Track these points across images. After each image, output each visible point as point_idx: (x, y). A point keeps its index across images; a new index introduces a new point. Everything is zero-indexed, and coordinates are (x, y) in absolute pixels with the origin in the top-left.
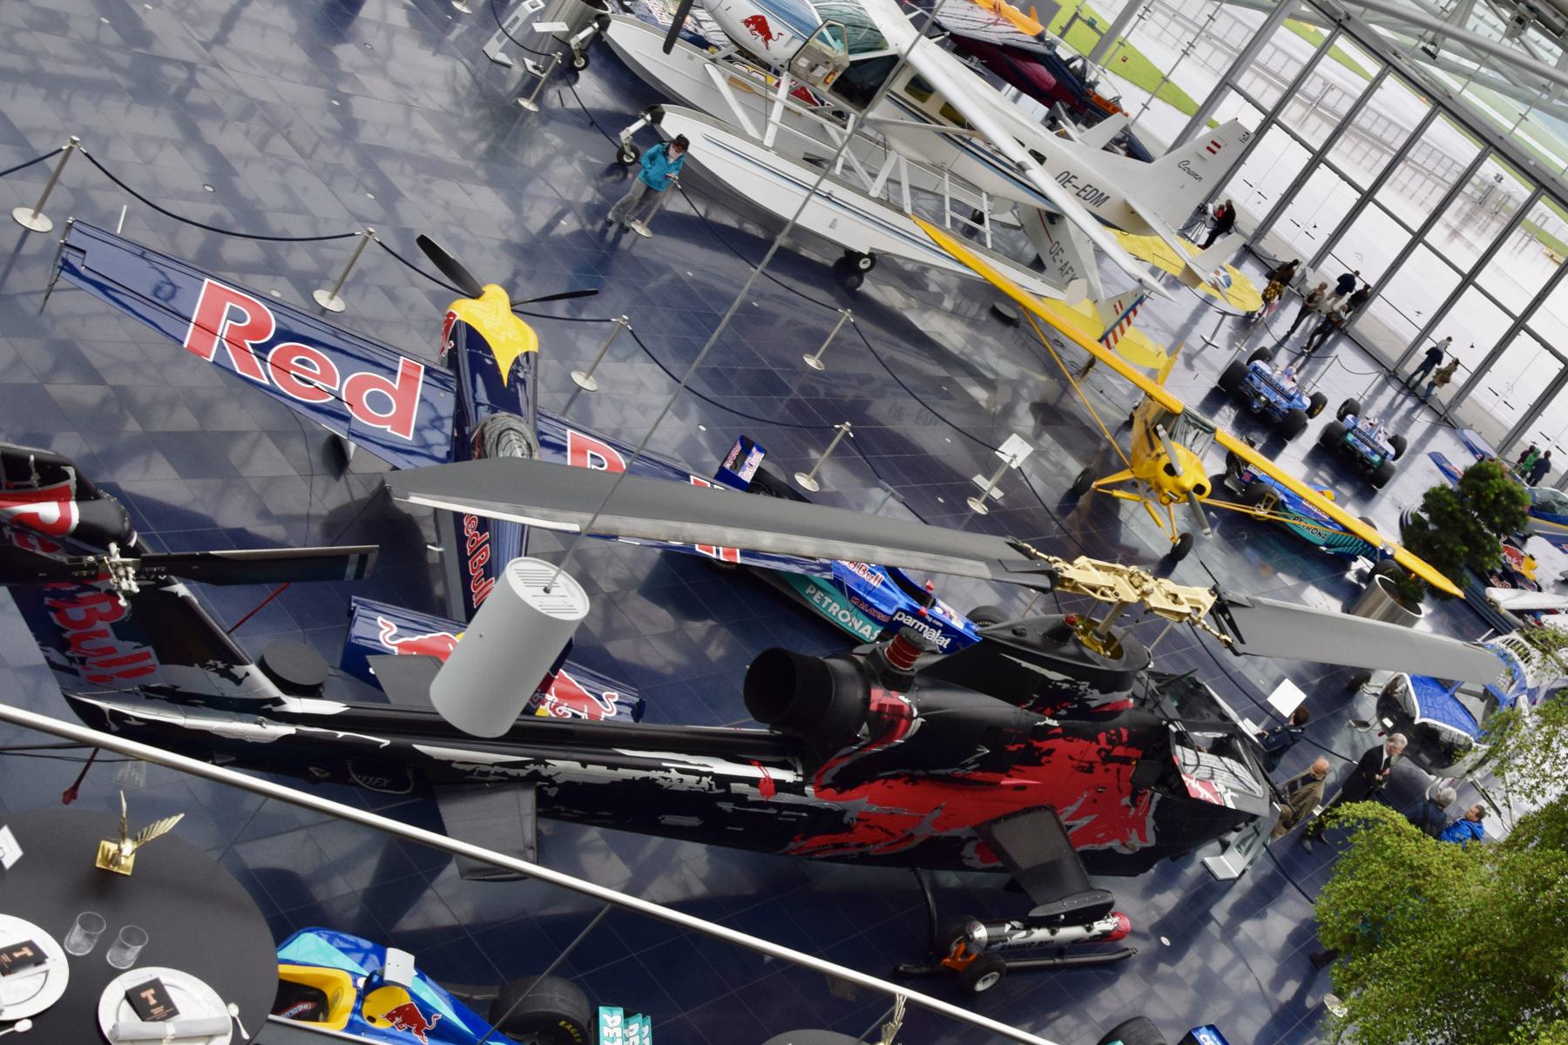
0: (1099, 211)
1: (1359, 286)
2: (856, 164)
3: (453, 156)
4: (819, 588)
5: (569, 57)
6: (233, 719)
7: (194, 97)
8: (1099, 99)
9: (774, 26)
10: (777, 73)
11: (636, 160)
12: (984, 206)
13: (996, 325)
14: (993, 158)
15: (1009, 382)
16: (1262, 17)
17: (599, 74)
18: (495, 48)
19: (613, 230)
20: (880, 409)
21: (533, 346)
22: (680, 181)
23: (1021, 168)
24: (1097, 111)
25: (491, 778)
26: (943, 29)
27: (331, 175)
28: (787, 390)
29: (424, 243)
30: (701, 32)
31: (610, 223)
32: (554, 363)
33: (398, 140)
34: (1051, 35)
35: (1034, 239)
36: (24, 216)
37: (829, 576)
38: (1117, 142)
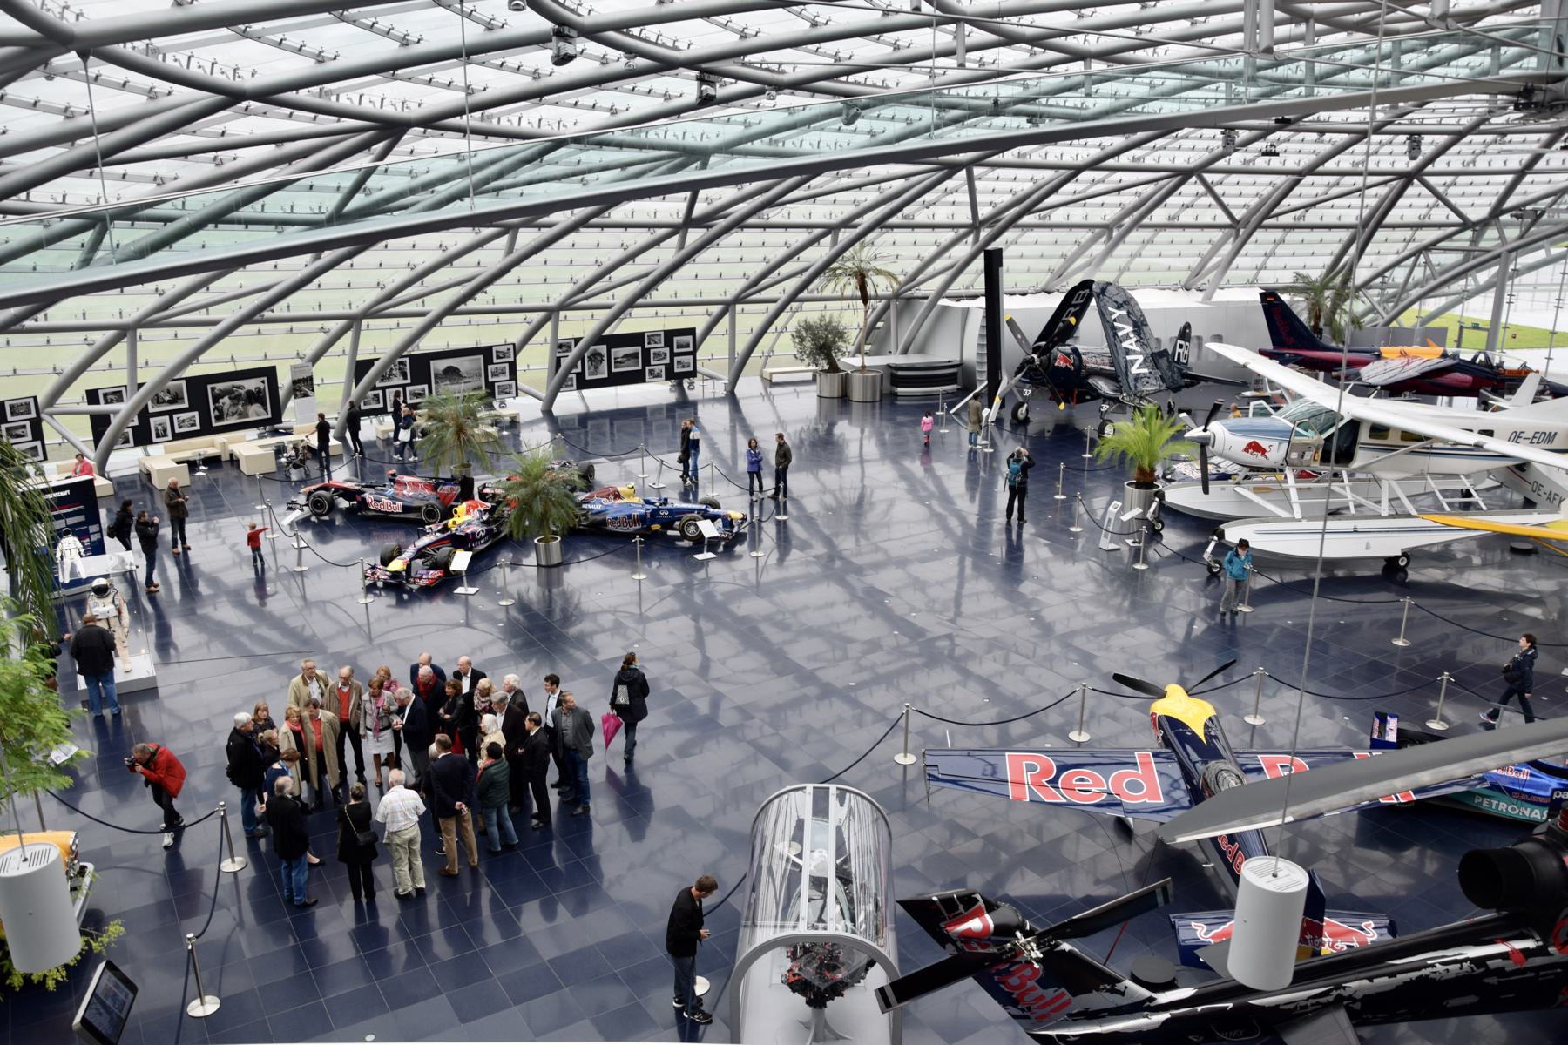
0: (1554, 446)
2: (1363, 501)
3: (1111, 617)
4: (1483, 796)
5: (1151, 526)
6: (1130, 1019)
7: (958, 652)
8: (1511, 372)
9: (1264, 443)
10: (1281, 470)
11: (1221, 568)
12: (1467, 484)
13: (1519, 558)
14: (1455, 450)
15: (1554, 593)
17: (1173, 527)
18: (1106, 544)
19: (1228, 617)
20: (1465, 653)
21: (1212, 713)
22: (1255, 567)
23: (1478, 446)
24: (1511, 380)
25: (1310, 1009)
26: (1375, 387)
27: (1050, 659)
28: (1392, 669)
29: (1119, 678)
30: (1221, 471)
31: (1224, 614)
32: (1231, 717)
33: (1078, 623)
34: (1451, 350)
35: (1517, 489)
36: (900, 759)
37: (1487, 785)
38: (1541, 393)
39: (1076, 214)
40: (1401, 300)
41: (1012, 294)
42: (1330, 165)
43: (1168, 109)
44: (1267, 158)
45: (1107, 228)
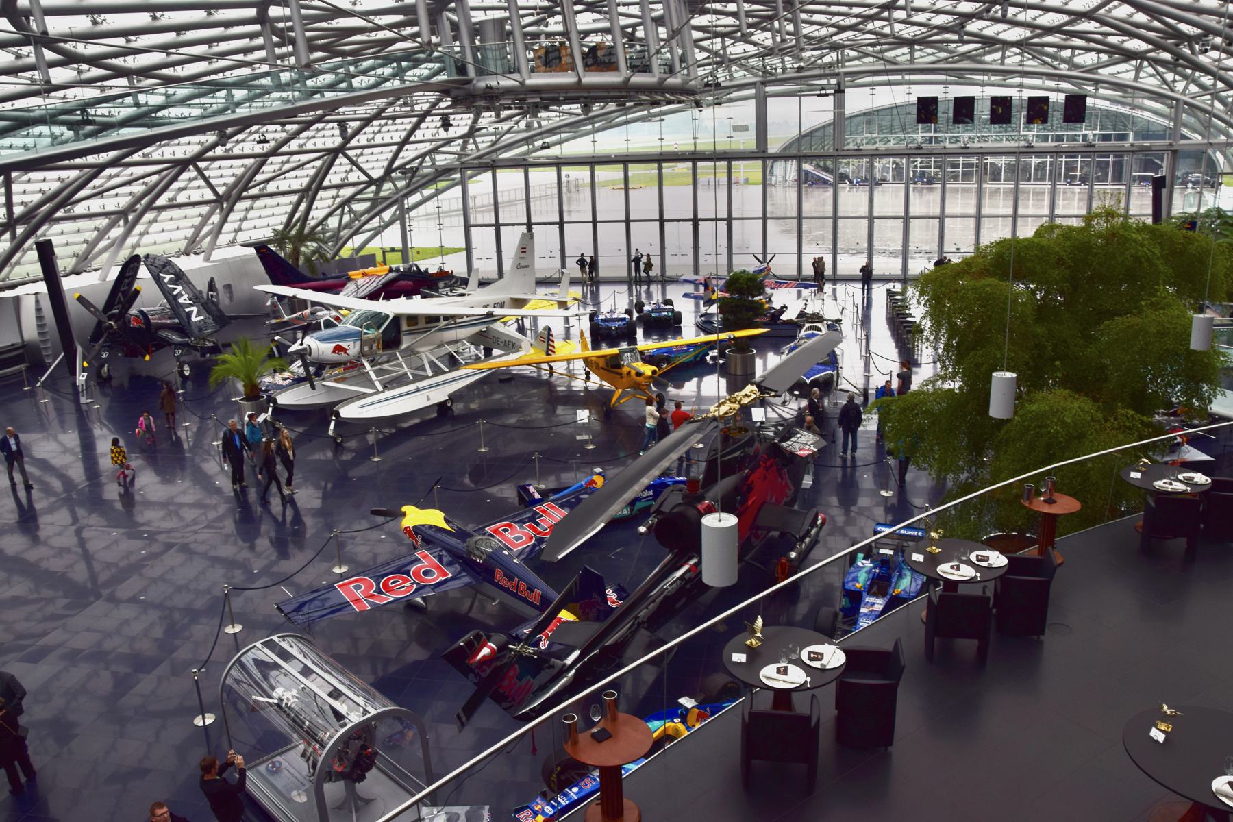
1: (588, 260)
16: (459, 188)
39: (95, 205)
40: (338, 239)
41: (68, 275)
42: (285, 149)
43: (242, 112)
44: (261, 145)
45: (122, 214)
